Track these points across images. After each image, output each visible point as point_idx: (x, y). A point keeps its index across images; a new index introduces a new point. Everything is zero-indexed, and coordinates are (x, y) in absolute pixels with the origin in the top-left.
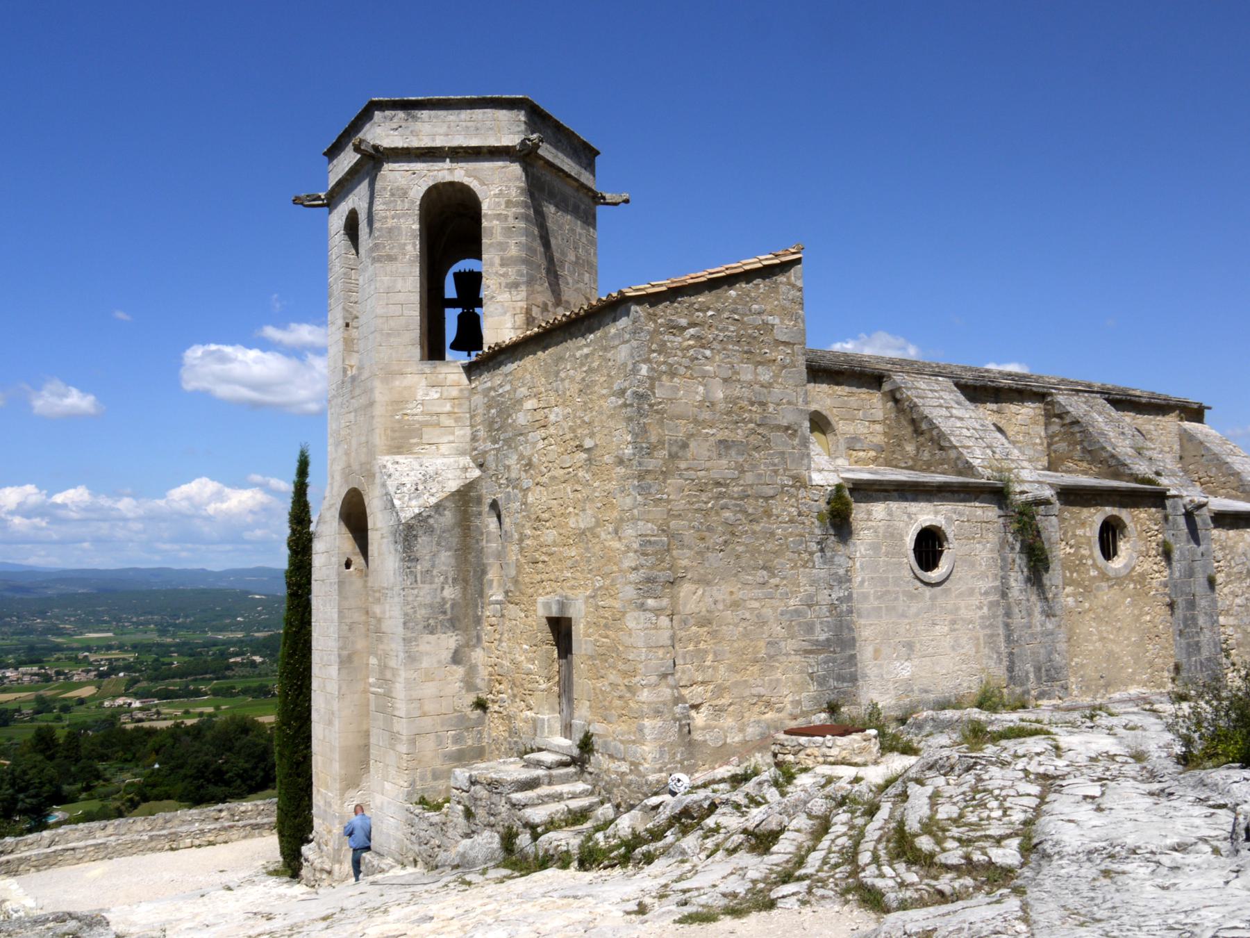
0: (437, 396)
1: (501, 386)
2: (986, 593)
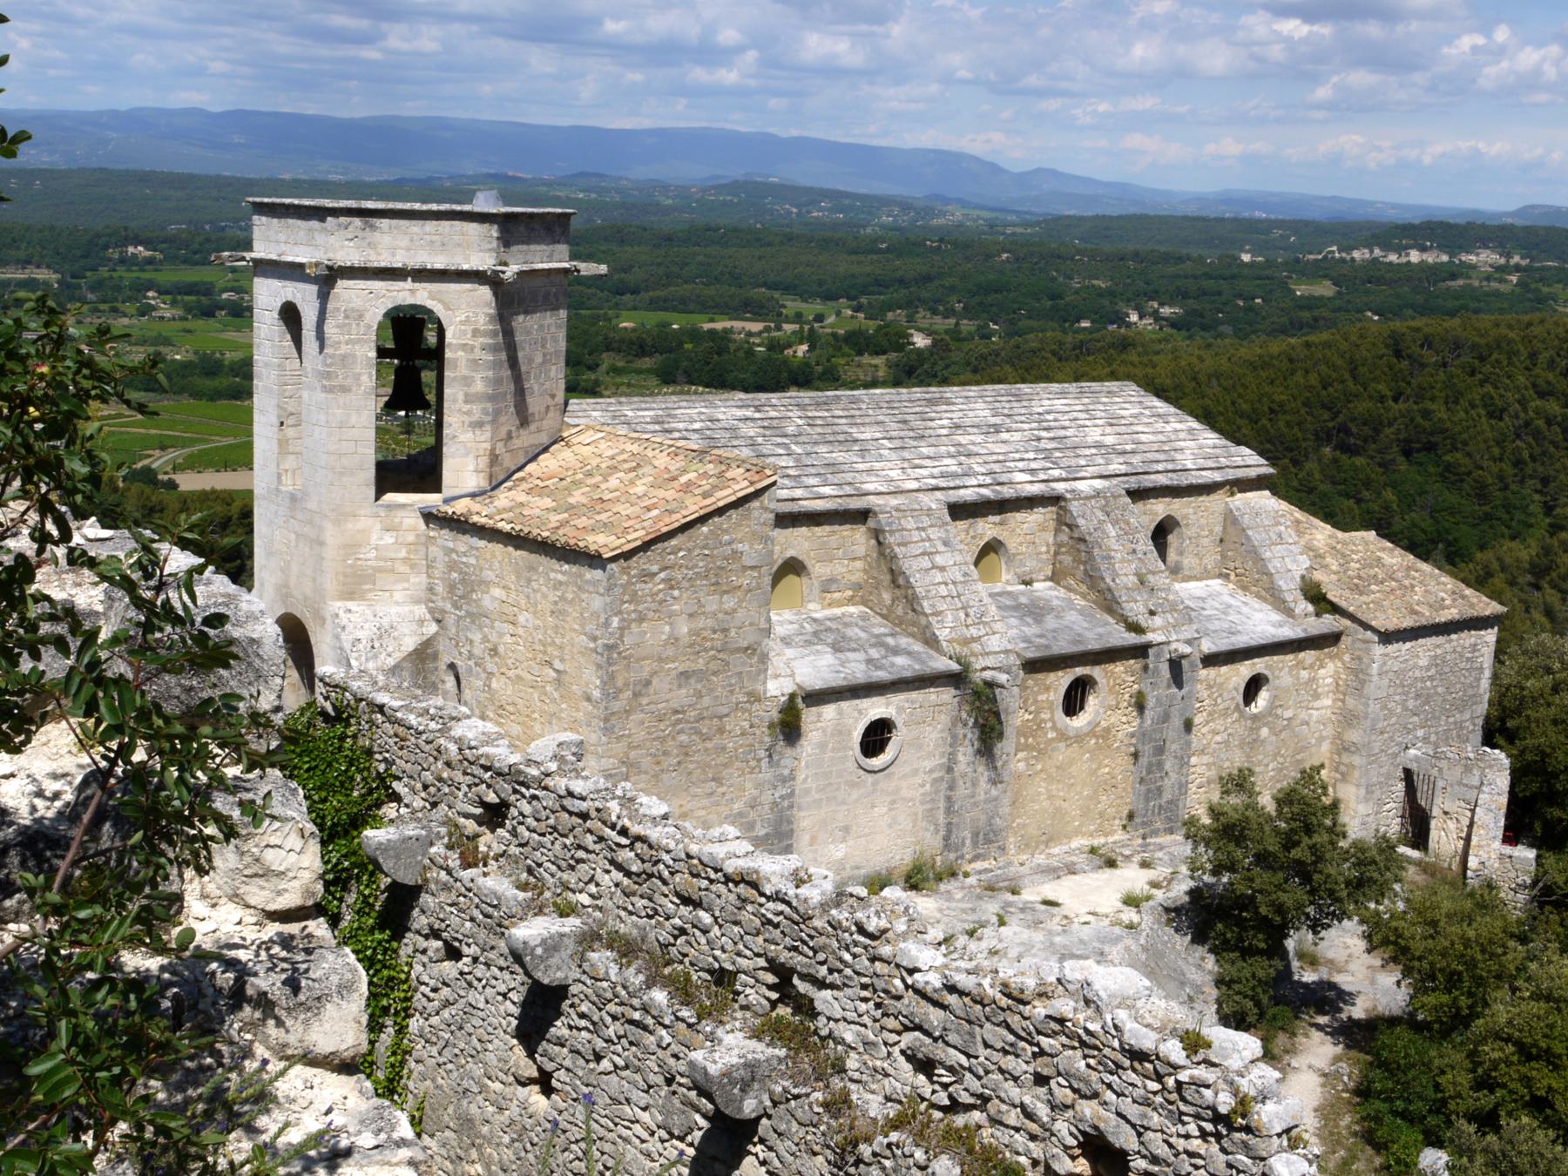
0: (392, 540)
2: (931, 771)
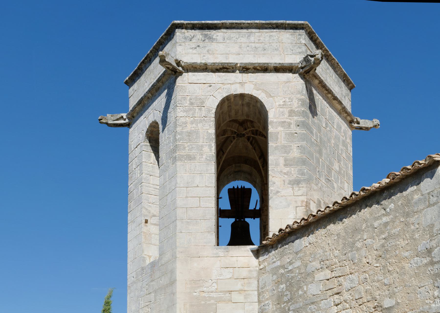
1: (290, 263)
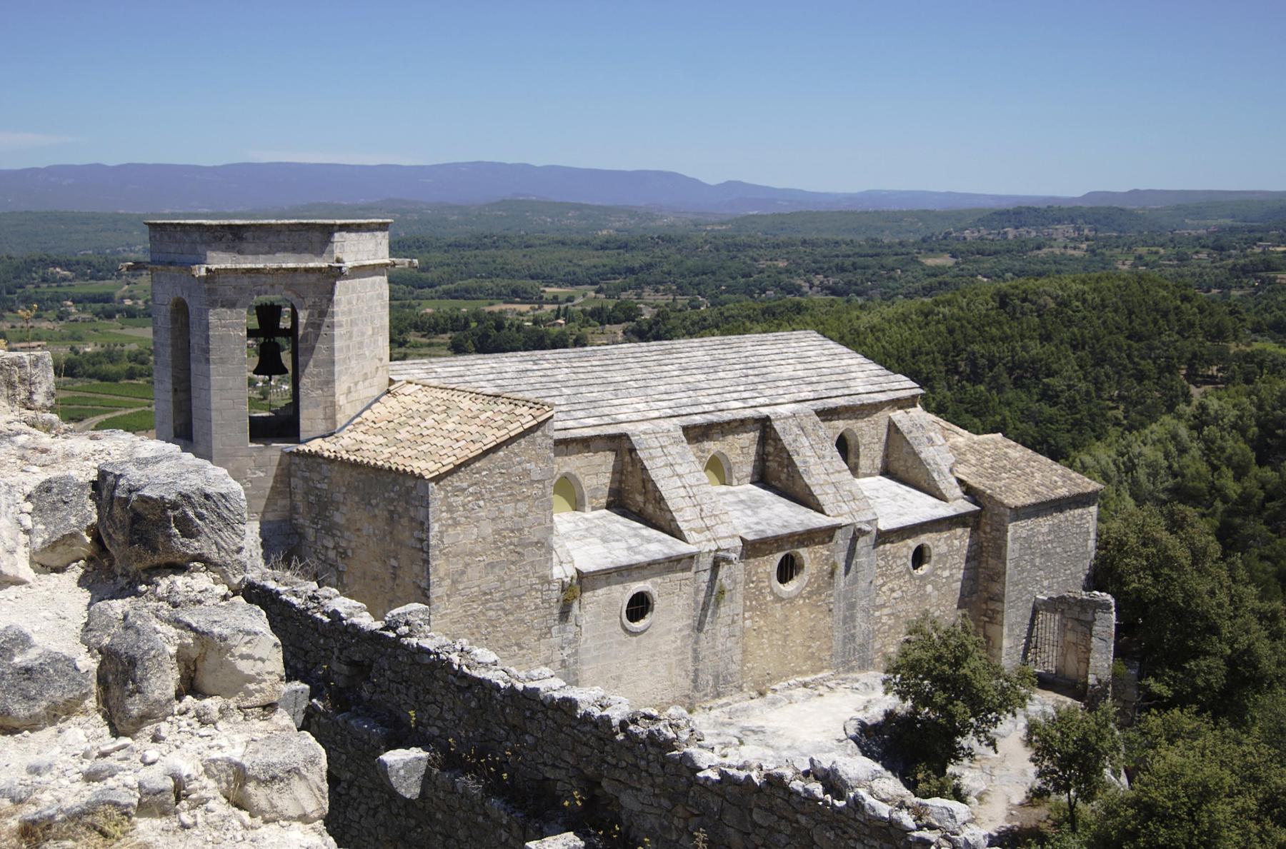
2: (681, 630)
